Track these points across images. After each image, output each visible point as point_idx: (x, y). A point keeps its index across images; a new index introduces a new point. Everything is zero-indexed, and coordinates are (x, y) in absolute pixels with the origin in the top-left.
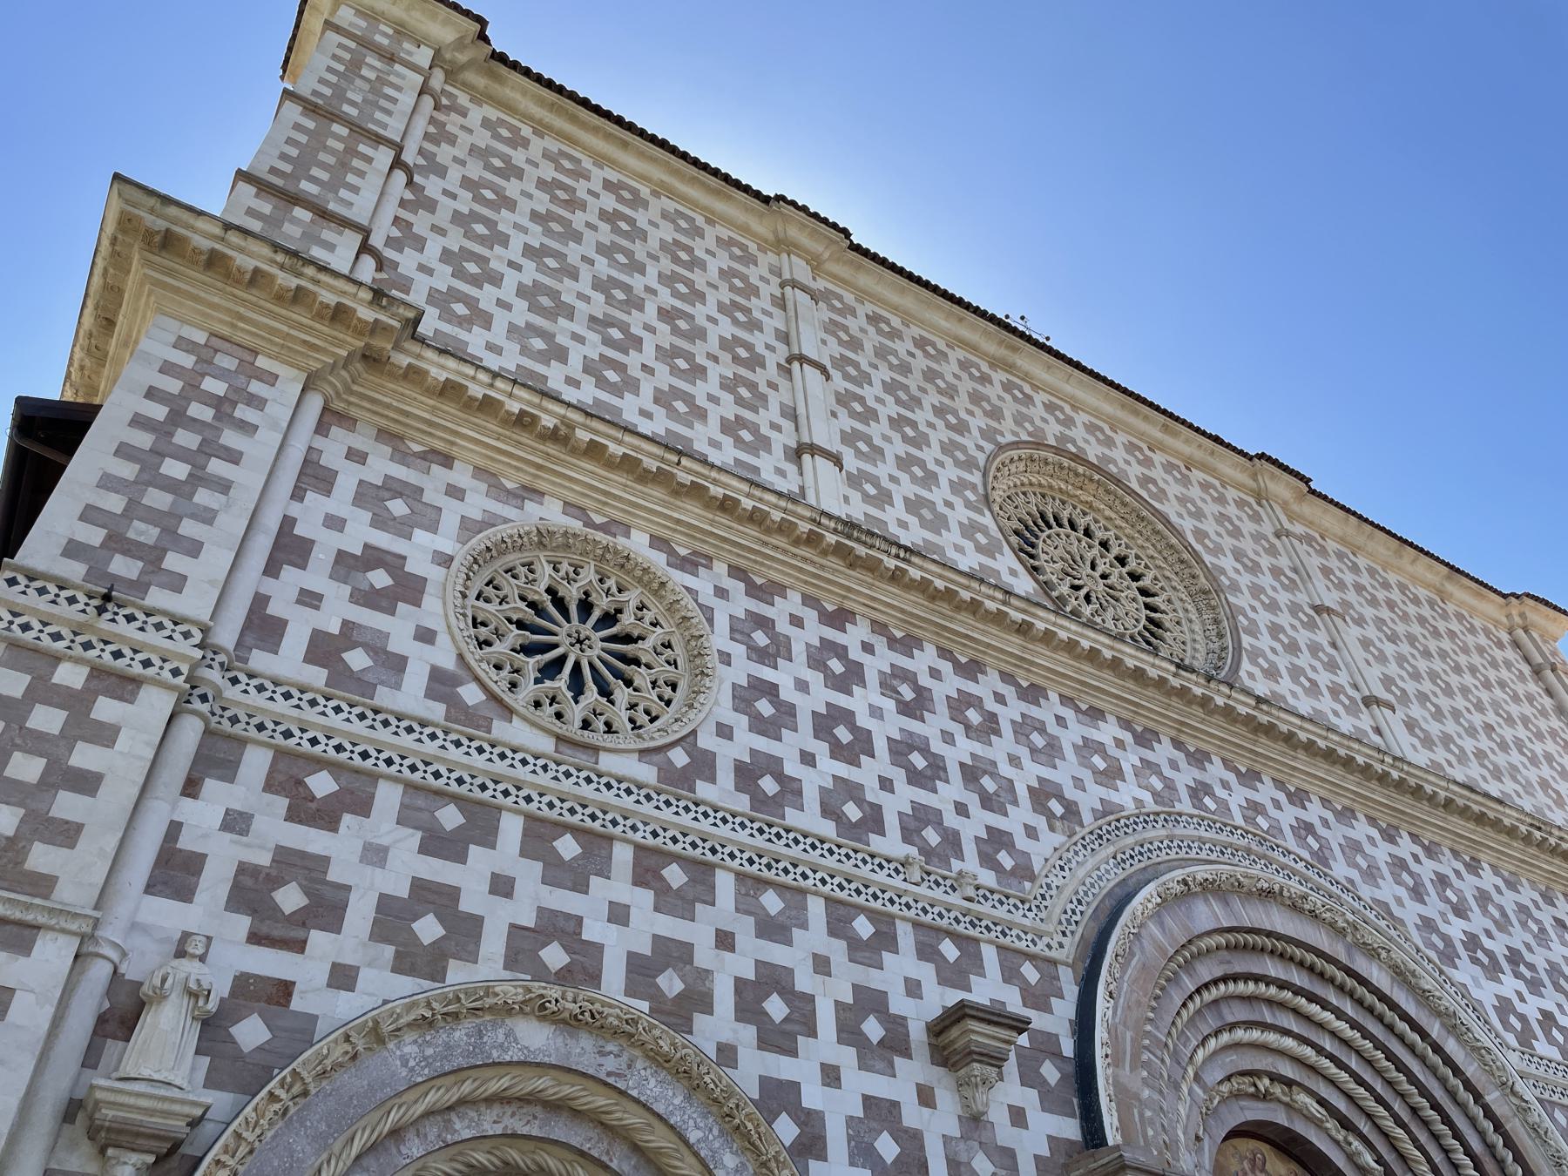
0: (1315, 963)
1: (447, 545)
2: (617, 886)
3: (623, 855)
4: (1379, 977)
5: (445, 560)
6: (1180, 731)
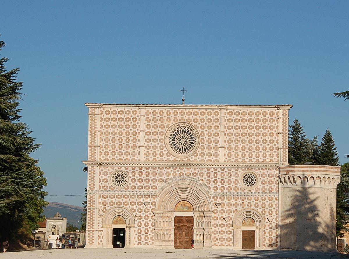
0: (188, 188)
1: (109, 175)
2: (122, 198)
3: (123, 196)
4: (195, 188)
5: (109, 177)
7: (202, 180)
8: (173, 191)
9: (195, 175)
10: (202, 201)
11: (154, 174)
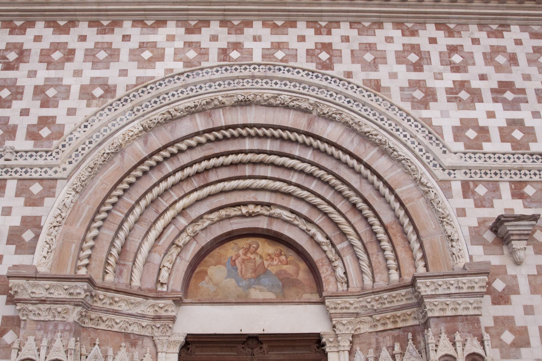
6: (224, 15)
7: (377, 86)
8: (174, 150)
9: (324, 56)
10: (387, 218)
11: (57, 56)
